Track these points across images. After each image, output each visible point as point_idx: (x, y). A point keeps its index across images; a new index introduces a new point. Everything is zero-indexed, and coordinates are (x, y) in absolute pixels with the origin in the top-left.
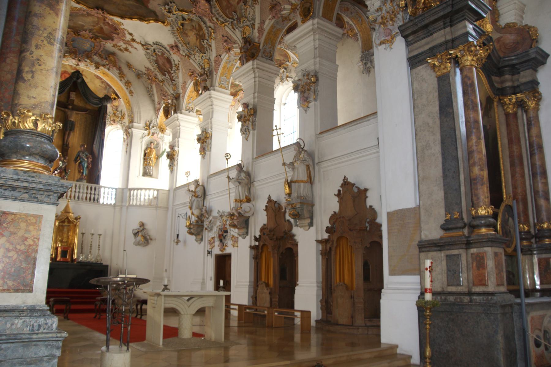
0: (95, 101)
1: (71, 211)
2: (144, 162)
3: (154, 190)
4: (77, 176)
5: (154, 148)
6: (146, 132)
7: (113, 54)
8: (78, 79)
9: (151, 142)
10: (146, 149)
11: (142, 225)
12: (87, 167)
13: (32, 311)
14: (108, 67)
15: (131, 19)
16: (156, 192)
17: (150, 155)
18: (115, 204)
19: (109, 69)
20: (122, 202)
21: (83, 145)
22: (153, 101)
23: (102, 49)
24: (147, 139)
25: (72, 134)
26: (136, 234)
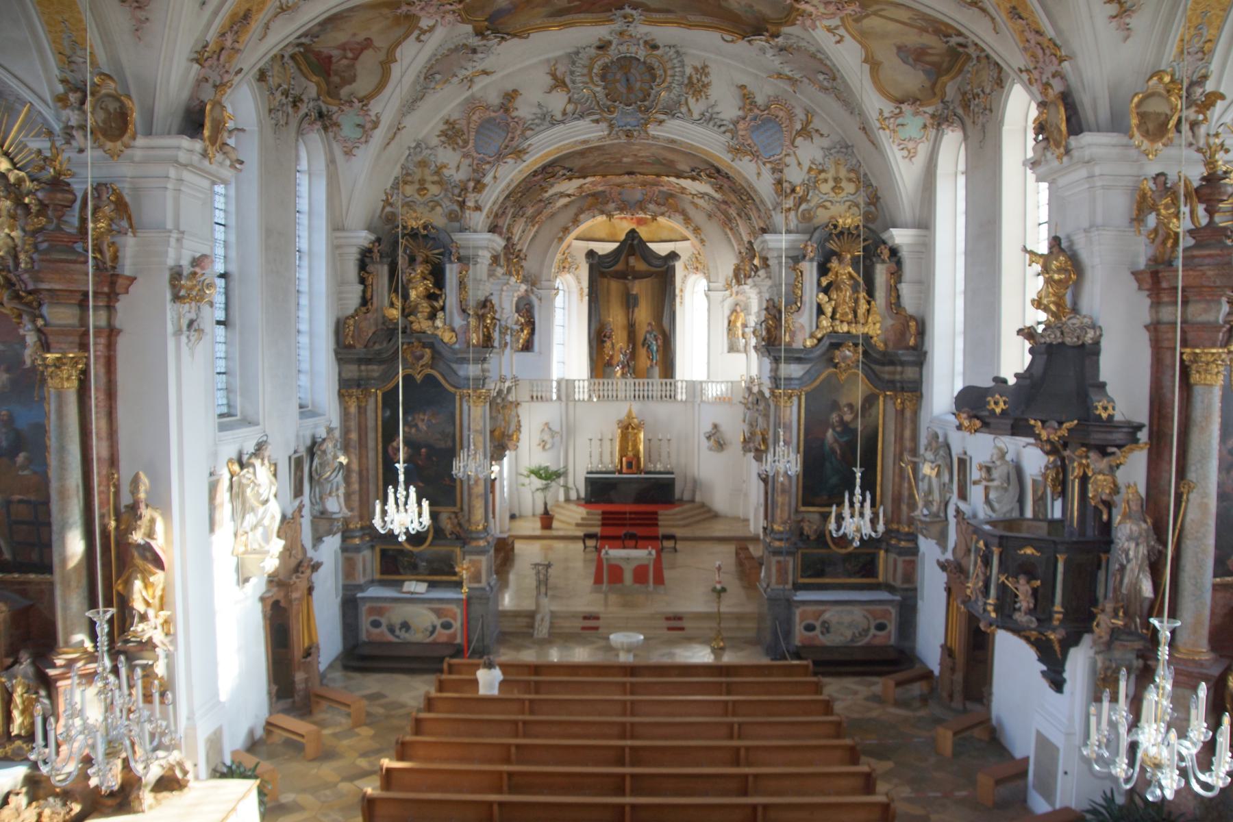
0: (658, 263)
1: (634, 415)
2: (728, 334)
3: (727, 382)
4: (649, 363)
5: (742, 311)
6: (728, 293)
7: (672, 196)
8: (633, 240)
9: (737, 305)
10: (729, 317)
11: (715, 426)
12: (657, 351)
13: (483, 589)
14: (667, 214)
15: (668, 176)
16: (730, 384)
17: (735, 322)
18: (686, 401)
19: (669, 217)
20: (694, 397)
21: (650, 324)
22: (733, 246)
23: (657, 193)
24: (729, 302)
25: (636, 310)
26: (709, 438)
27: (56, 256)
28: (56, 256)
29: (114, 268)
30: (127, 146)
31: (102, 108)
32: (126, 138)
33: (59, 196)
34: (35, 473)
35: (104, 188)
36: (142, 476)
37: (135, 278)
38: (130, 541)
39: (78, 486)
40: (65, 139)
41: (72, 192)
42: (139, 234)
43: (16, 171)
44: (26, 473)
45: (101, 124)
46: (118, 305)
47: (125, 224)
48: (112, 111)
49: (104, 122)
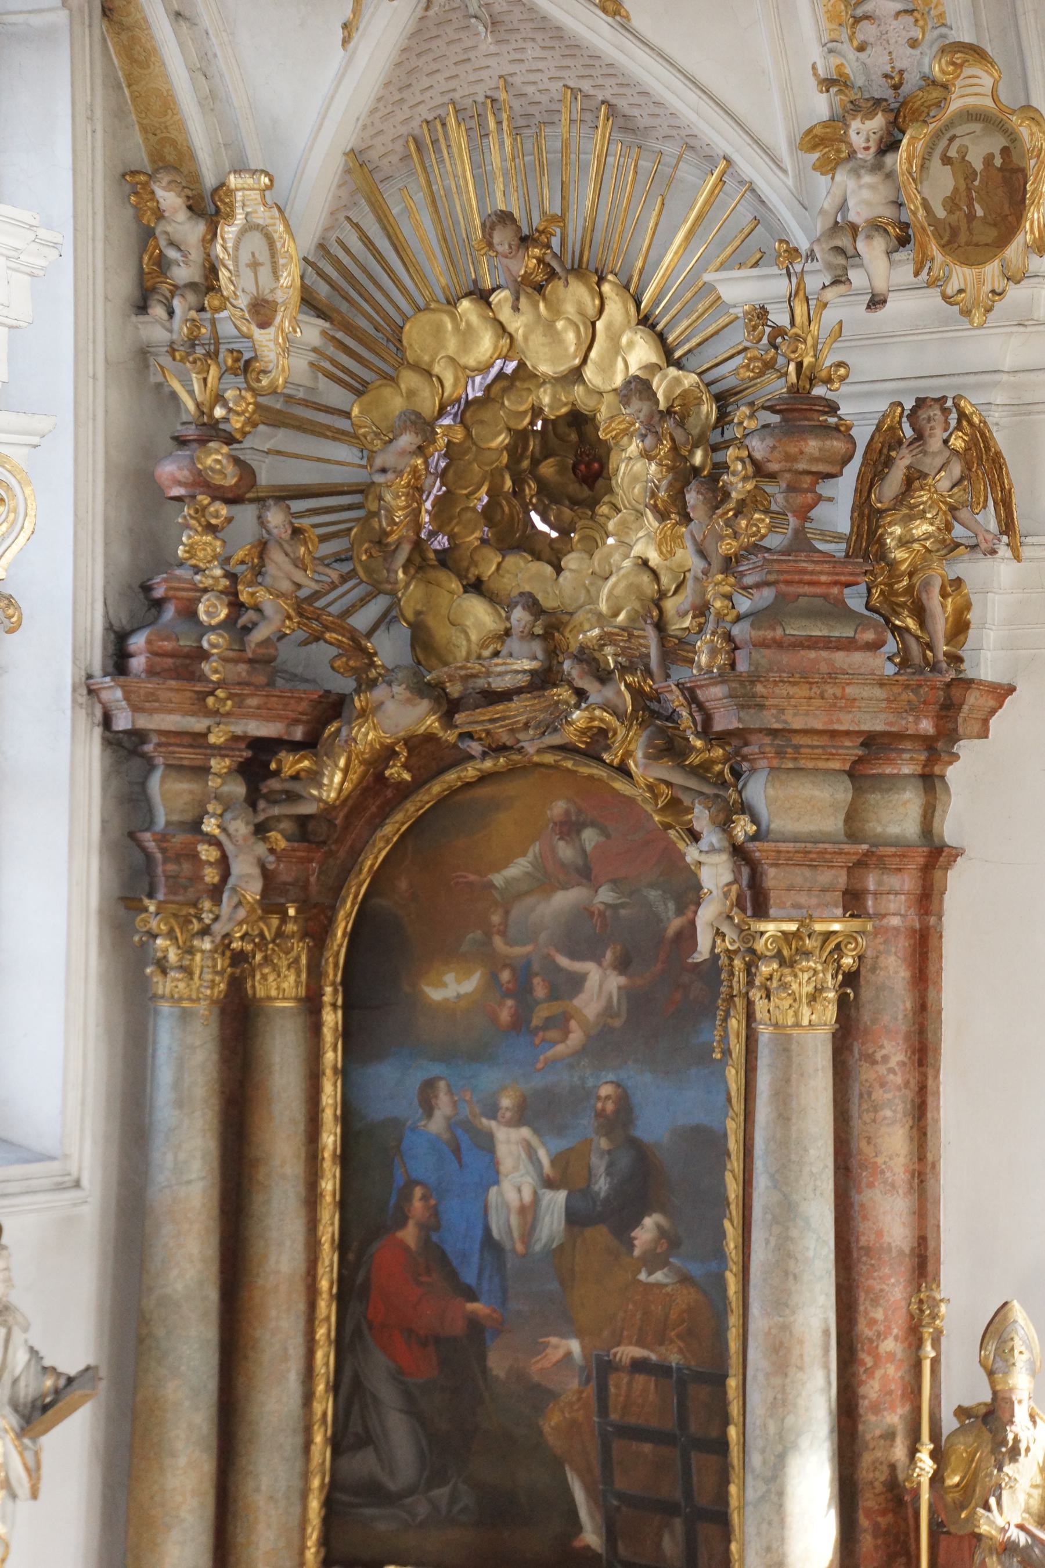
27: (797, 629)
28: (797, 629)
29: (956, 660)
30: (1016, 277)
31: (946, 160)
32: (1013, 251)
33: (812, 445)
34: (685, 1279)
35: (936, 412)
36: (1019, 1313)
37: (1011, 689)
38: (984, 1529)
39: (826, 1332)
40: (829, 266)
41: (842, 431)
42: (1025, 552)
43: (673, 371)
44: (659, 1276)
45: (941, 213)
46: (953, 773)
47: (989, 519)
48: (978, 166)
49: (951, 203)
